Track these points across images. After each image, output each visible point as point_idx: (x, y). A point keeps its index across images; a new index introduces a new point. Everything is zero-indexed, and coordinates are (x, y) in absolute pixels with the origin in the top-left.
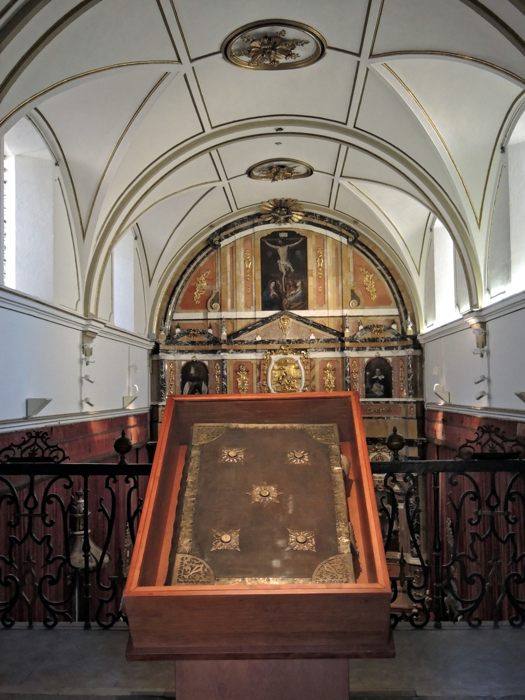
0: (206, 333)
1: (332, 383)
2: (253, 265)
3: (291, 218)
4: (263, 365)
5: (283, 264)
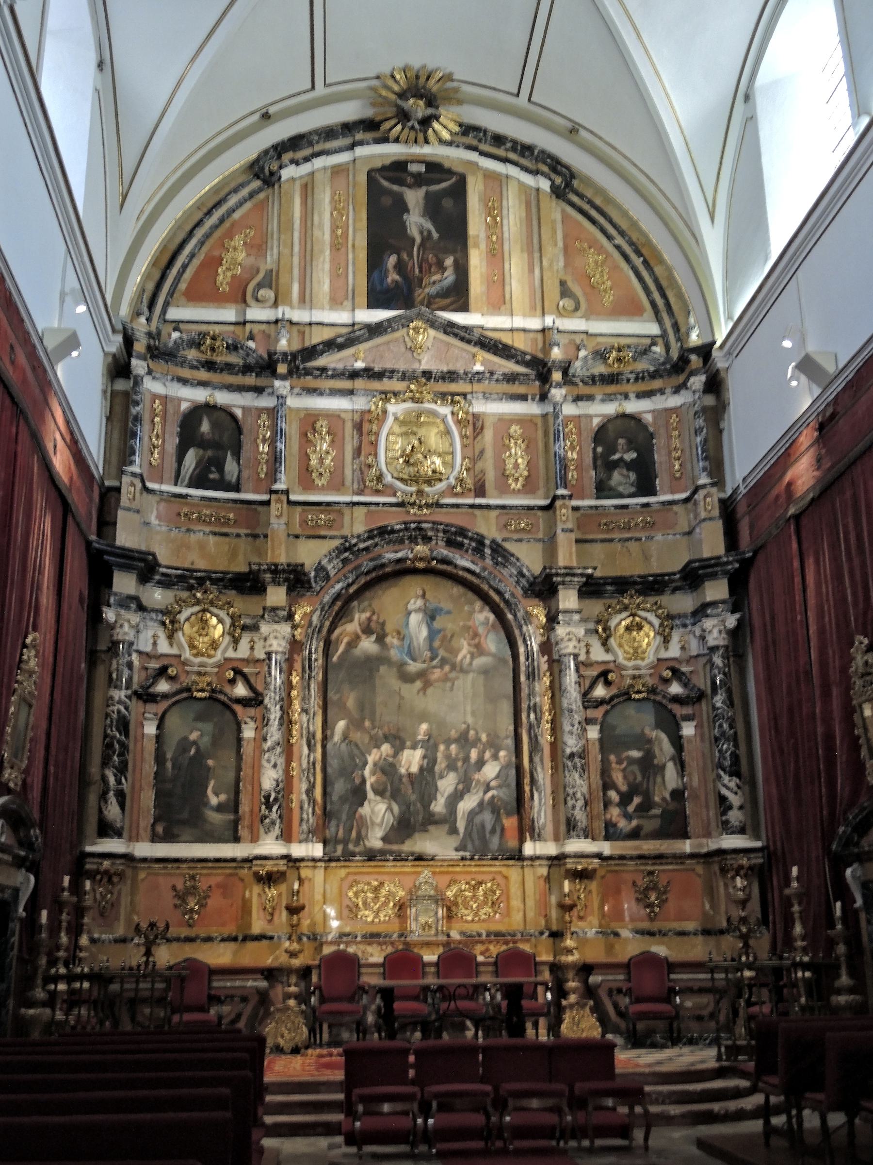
0: (242, 348)
1: (522, 467)
2: (351, 221)
3: (437, 118)
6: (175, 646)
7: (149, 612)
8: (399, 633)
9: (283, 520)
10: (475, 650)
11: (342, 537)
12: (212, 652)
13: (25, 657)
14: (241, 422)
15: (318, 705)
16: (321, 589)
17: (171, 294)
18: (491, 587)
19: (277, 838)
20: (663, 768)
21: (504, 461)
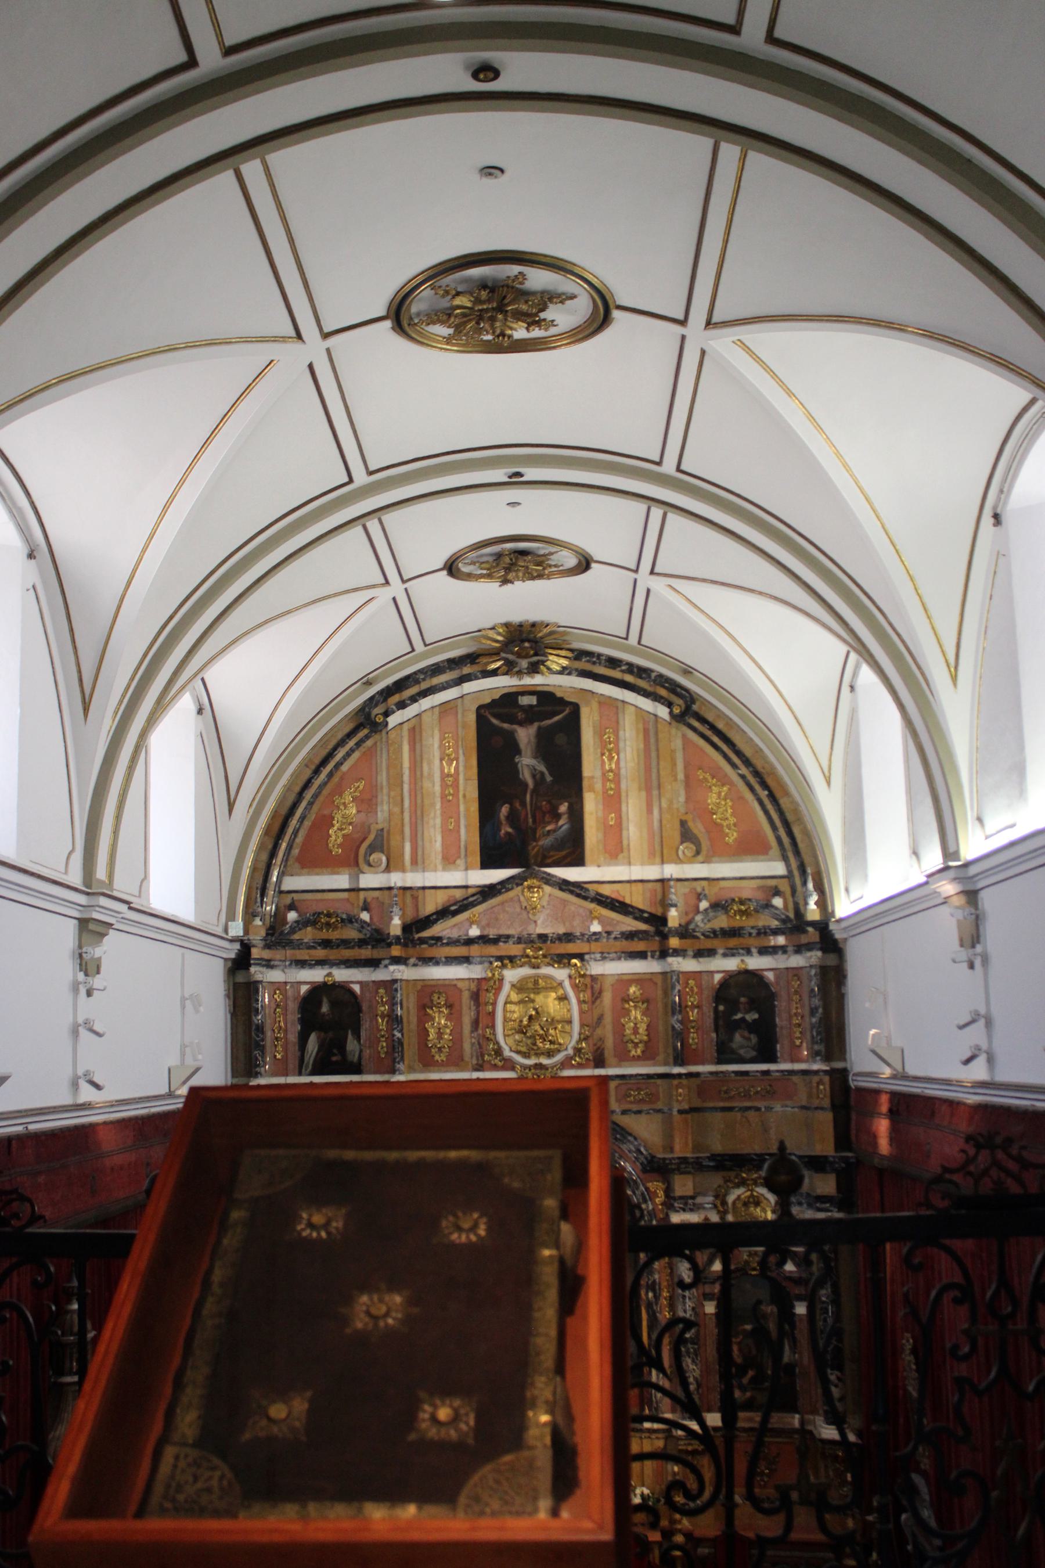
0: (356, 921)
1: (641, 1031)
2: (461, 769)
3: (543, 663)
4: (484, 992)
5: (528, 763)
14: (359, 998)
21: (624, 1025)
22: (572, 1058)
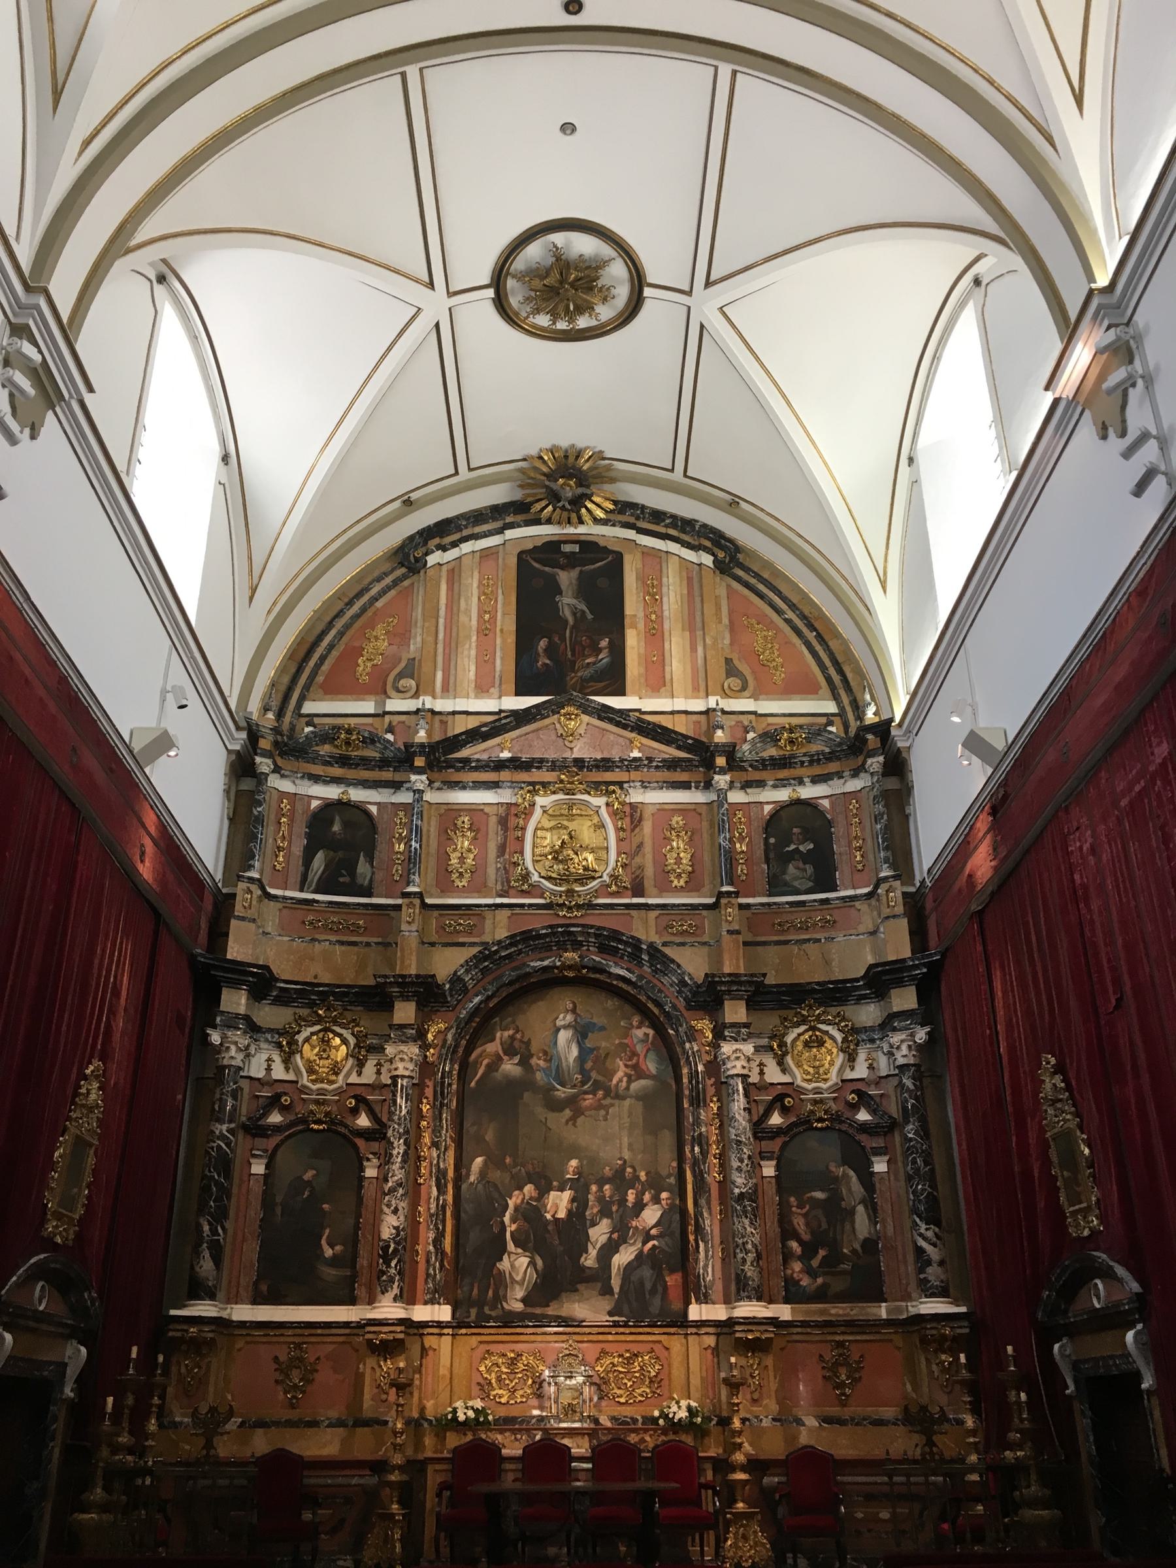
1: (684, 861)
2: (499, 606)
3: (589, 497)
4: (513, 818)
5: (568, 602)
6: (291, 1071)
7: (264, 1033)
8: (545, 1053)
9: (414, 927)
10: (633, 1073)
11: (483, 944)
12: (334, 1078)
13: (83, 1091)
15: (451, 1137)
16: (459, 1001)
17: (307, 687)
18: (649, 997)
19: (395, 1300)
20: (852, 1213)
22: (609, 886)
